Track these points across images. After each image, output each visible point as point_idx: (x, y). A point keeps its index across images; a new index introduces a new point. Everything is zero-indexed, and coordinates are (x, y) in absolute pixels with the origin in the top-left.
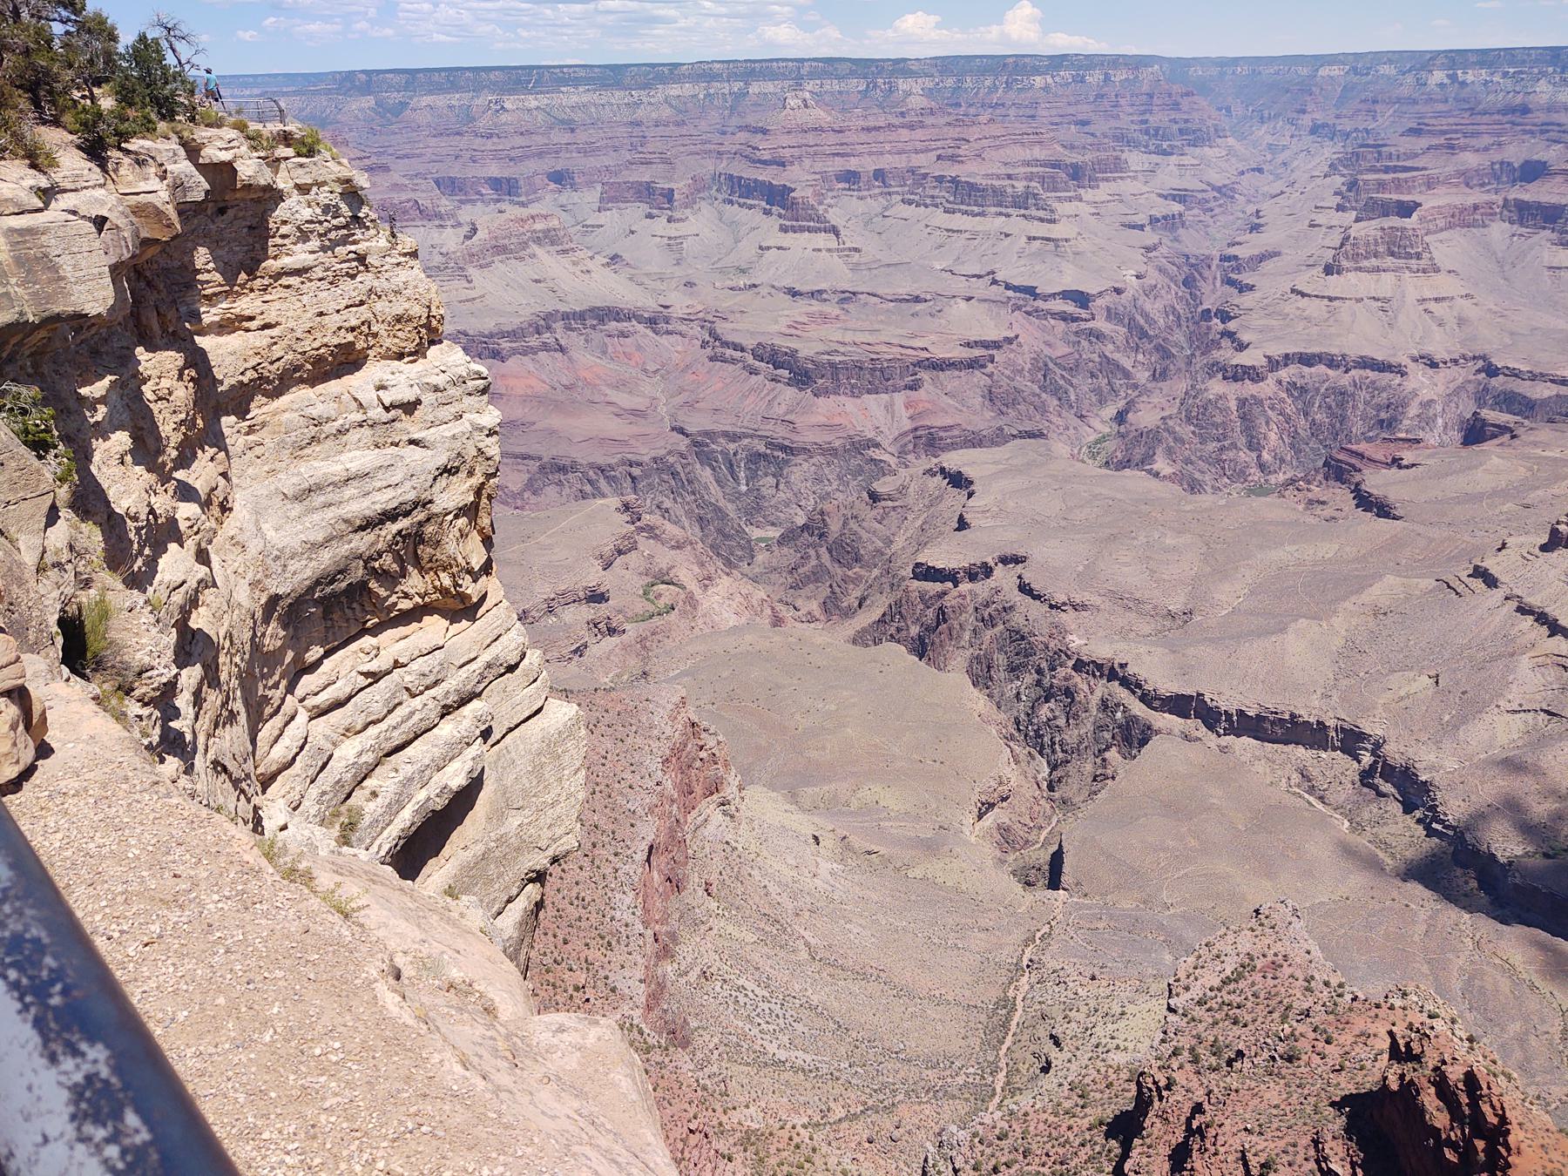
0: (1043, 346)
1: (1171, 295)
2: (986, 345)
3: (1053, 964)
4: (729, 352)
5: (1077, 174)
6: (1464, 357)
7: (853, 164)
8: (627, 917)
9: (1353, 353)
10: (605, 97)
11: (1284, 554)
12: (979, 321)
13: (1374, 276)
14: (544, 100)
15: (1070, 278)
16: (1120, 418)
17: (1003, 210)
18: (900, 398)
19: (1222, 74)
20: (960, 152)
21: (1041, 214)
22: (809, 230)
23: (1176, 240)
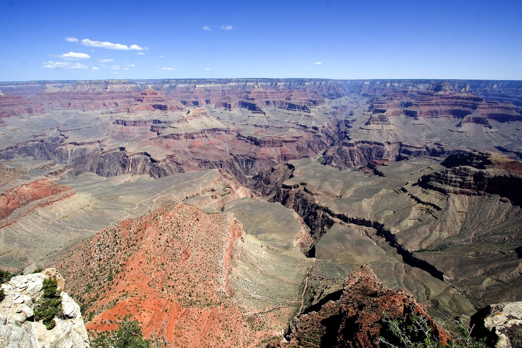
1: (335, 128)
2: (296, 138)
3: (313, 275)
5: (315, 103)
7: (268, 100)
8: (221, 266)
9: (373, 141)
10: (217, 85)
11: (361, 184)
12: (295, 132)
14: (204, 86)
15: (314, 124)
16: (324, 154)
18: (278, 148)
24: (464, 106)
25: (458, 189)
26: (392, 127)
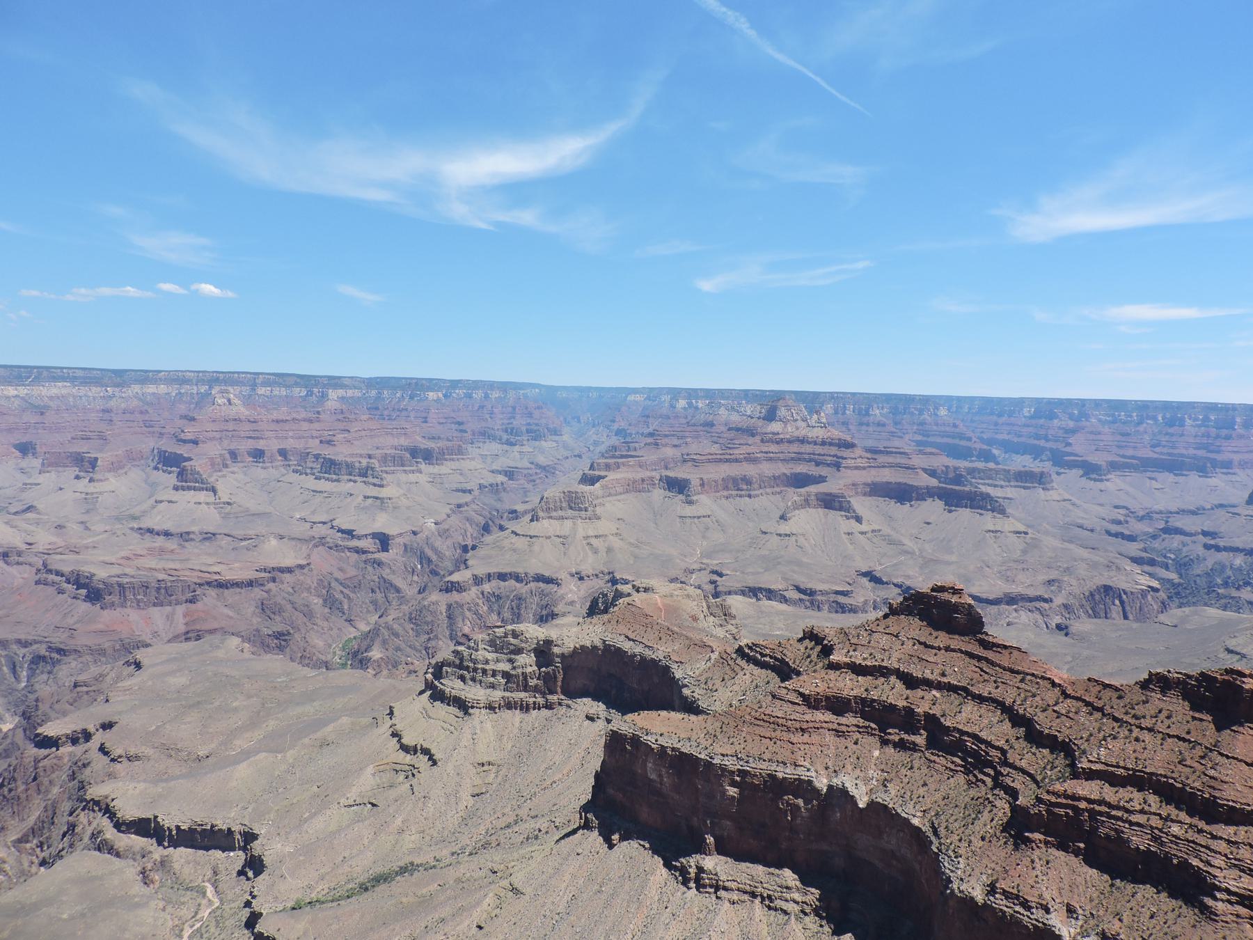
2: (282, 570)
4: (52, 577)
5: (427, 456)
7: (261, 444)
10: (83, 390)
13: (560, 522)
14: (23, 391)
15: (382, 523)
18: (180, 610)
21: (375, 481)
22: (195, 489)
24: (817, 464)
25: (497, 695)
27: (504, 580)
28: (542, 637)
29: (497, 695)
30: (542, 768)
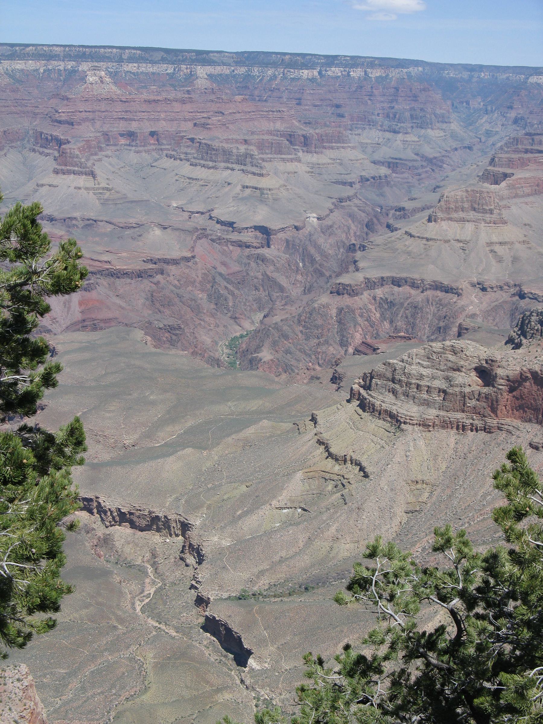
0: (218, 265)
2: (167, 261)
5: (306, 142)
6: (507, 284)
7: (134, 126)
15: (261, 215)
17: (230, 166)
19: (471, 77)
20: (209, 121)
21: (254, 169)
23: (382, 195)
25: (432, 413)
26: (510, 233)
27: (399, 286)
28: (484, 356)
29: (432, 413)
30: (481, 493)
